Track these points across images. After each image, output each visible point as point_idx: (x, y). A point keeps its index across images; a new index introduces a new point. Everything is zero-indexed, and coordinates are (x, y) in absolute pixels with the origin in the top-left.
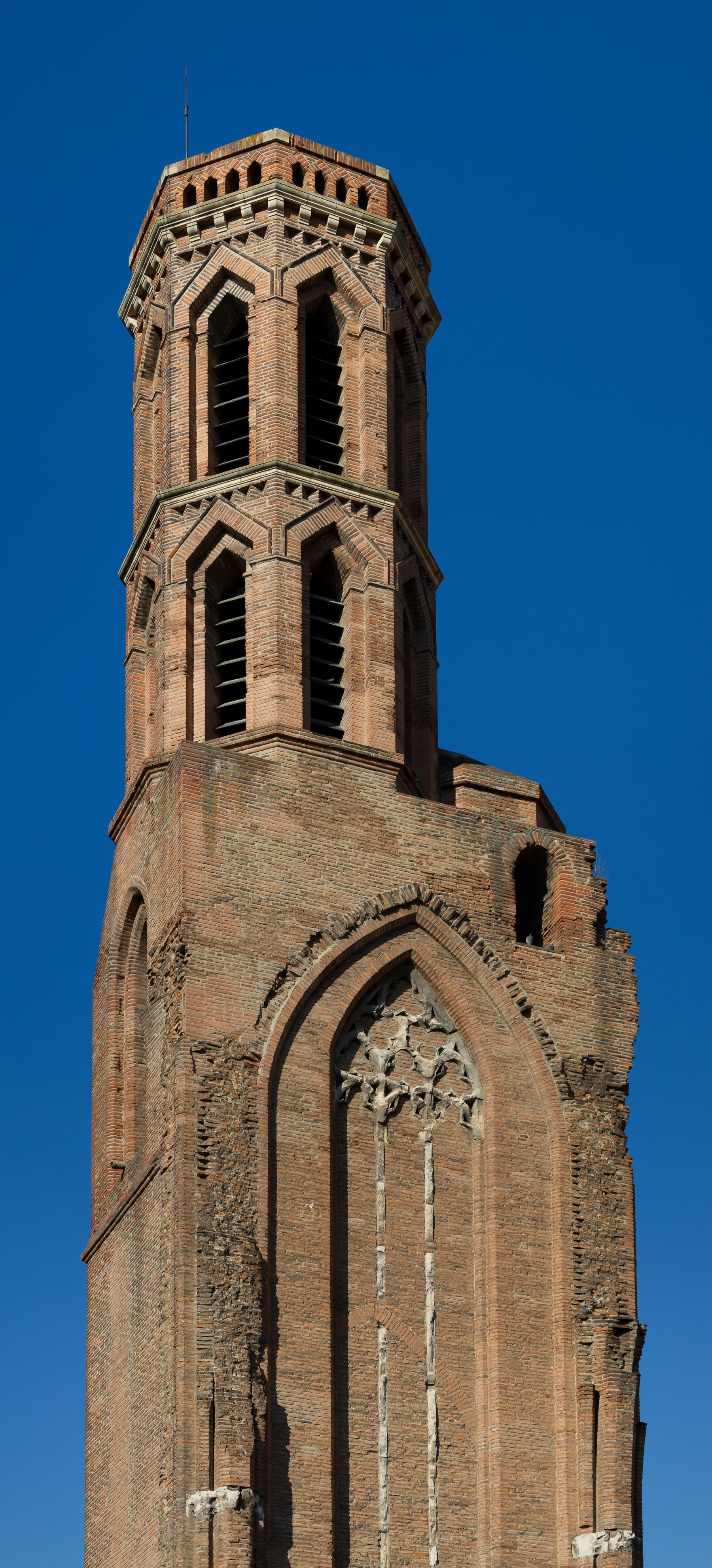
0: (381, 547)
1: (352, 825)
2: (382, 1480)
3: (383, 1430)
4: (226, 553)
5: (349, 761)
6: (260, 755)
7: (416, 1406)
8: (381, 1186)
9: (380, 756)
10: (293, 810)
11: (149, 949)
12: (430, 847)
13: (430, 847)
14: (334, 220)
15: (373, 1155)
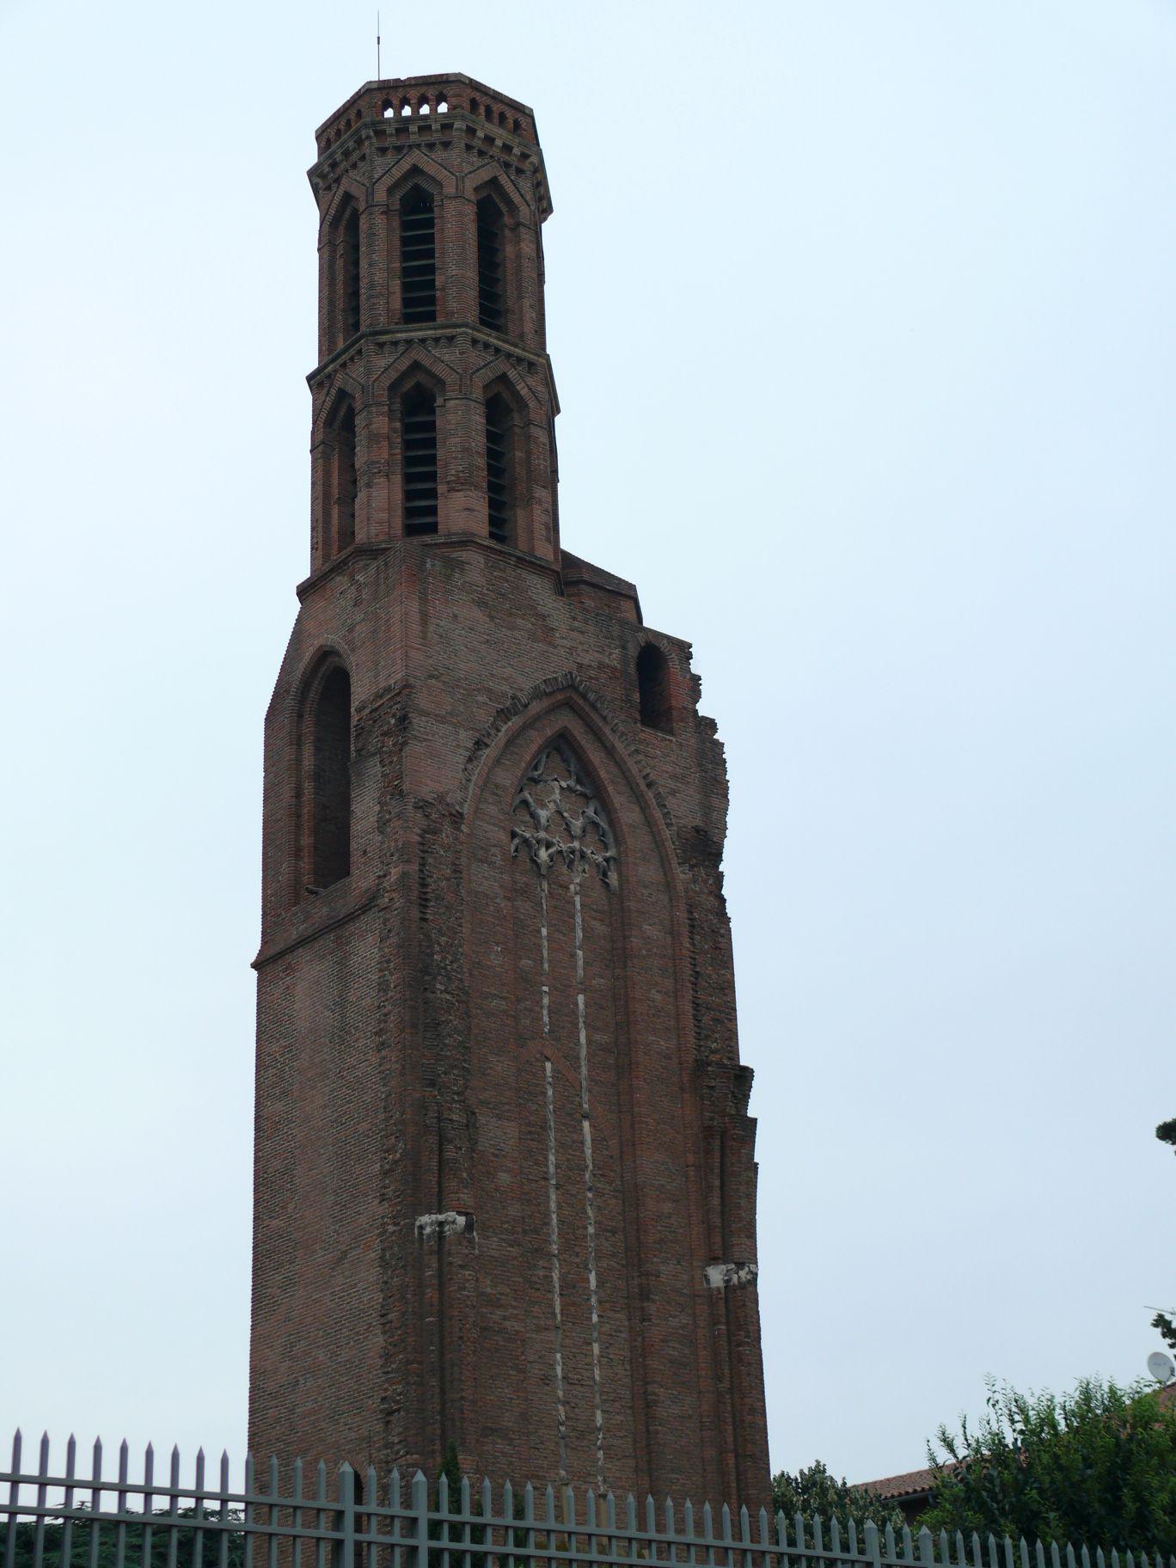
2: (553, 1206)
4: (418, 386)
6: (454, 555)
7: (575, 1136)
8: (544, 931)
10: (481, 603)
11: (354, 705)
14: (499, 143)
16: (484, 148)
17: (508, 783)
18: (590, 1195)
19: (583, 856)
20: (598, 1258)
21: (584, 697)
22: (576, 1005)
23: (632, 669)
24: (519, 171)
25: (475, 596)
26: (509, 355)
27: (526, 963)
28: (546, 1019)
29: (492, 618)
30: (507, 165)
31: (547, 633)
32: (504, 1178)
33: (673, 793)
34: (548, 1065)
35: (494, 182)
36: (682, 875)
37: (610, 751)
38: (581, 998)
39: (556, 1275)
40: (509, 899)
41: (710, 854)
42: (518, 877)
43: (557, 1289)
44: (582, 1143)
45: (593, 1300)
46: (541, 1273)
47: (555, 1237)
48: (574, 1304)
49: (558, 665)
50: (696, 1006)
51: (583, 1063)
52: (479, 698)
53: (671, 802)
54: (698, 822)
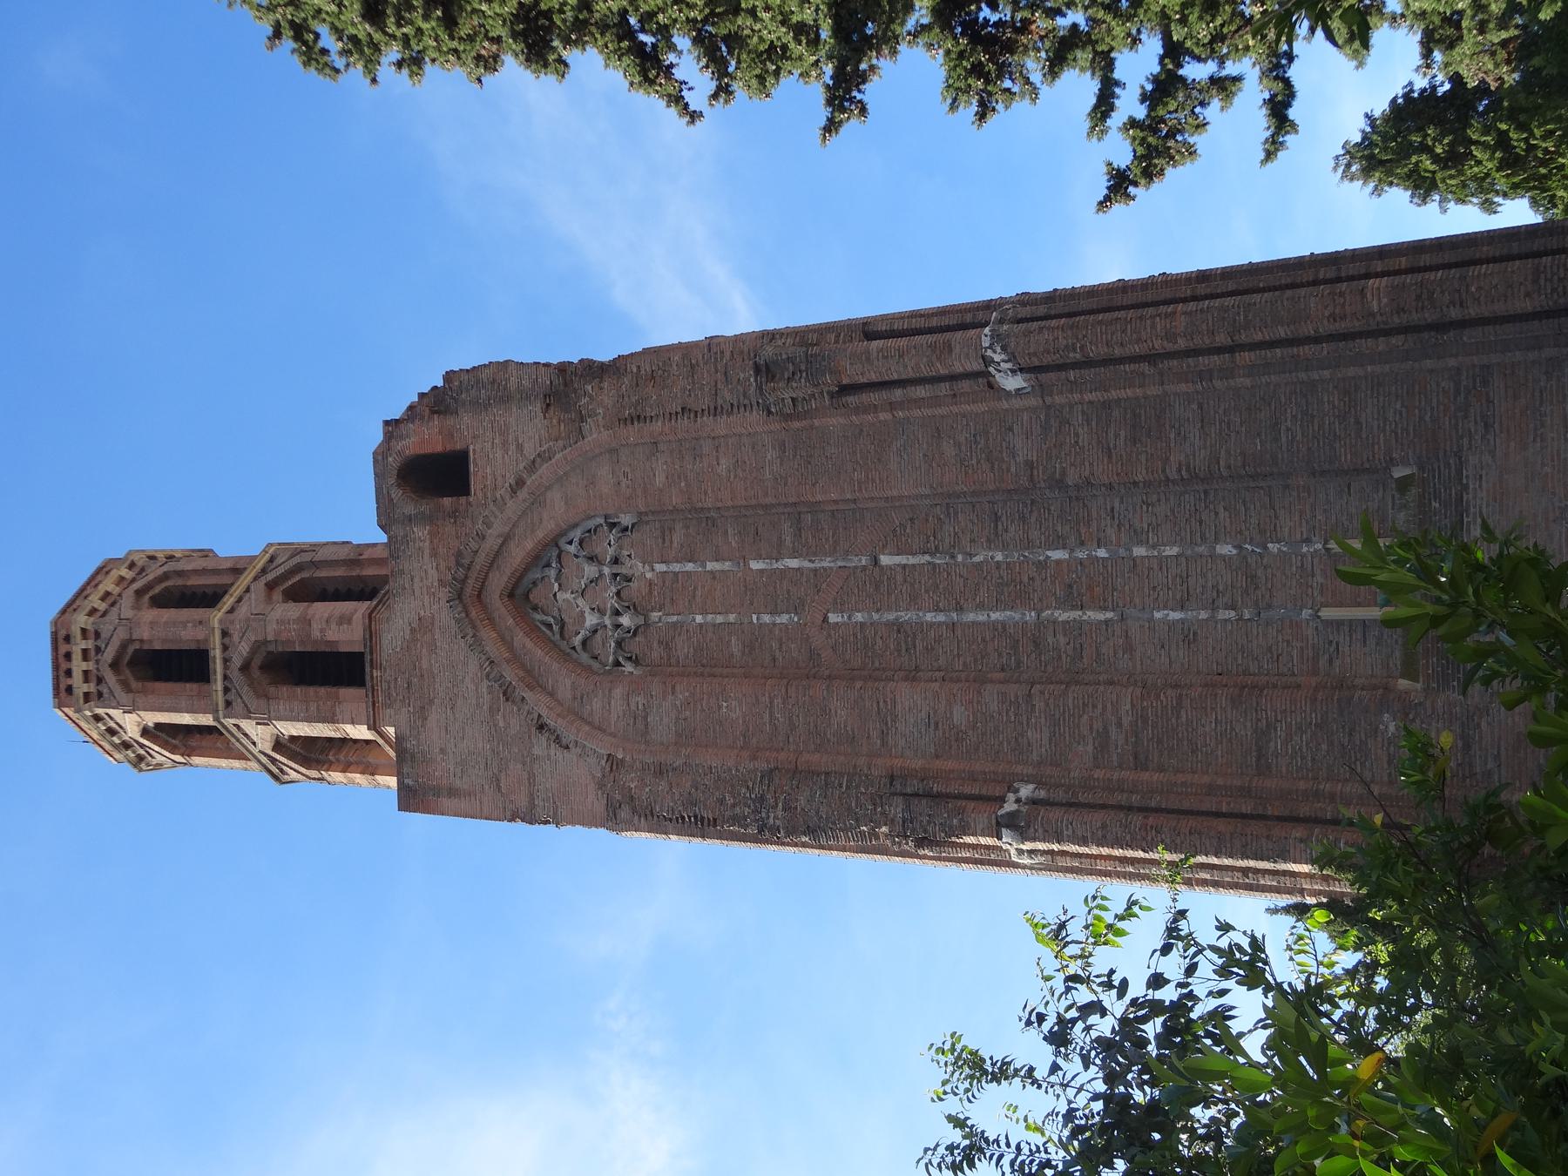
2: (981, 617)
3: (929, 617)
7: (899, 578)
8: (699, 619)
10: (422, 713)
14: (84, 666)
15: (674, 624)
17: (568, 682)
18: (960, 558)
19: (616, 561)
20: (1029, 545)
21: (463, 581)
22: (762, 571)
23: (425, 507)
24: (97, 635)
25: (419, 723)
26: (226, 661)
27: (735, 647)
28: (784, 619)
29: (431, 702)
30: (98, 650)
31: (423, 626)
32: (959, 715)
33: (520, 447)
34: (833, 618)
35: (115, 666)
36: (596, 435)
37: (507, 539)
38: (755, 565)
39: (1063, 616)
40: (673, 687)
41: (566, 385)
42: (655, 655)
43: (1076, 614)
44: (904, 567)
45: (1081, 554)
46: (1062, 640)
47: (1017, 616)
48: (1090, 588)
49: (445, 617)
50: (715, 411)
51: (817, 565)
52: (501, 724)
53: (530, 451)
54: (538, 407)
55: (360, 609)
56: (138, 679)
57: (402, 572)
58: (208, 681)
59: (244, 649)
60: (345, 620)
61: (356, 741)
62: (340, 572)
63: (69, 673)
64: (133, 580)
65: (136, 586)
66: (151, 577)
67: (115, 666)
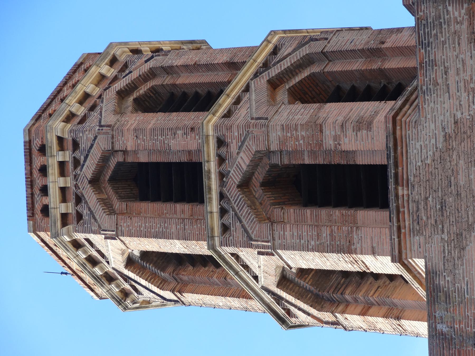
0: (242, 138)
1: (458, 174)
5: (405, 177)
9: (391, 145)
10: (459, 242)
12: (457, 78)
13: (457, 78)
14: (61, 182)
16: (72, 198)
24: (76, 145)
25: (456, 254)
26: (222, 176)
30: (76, 163)
55: (381, 110)
56: (121, 198)
57: (434, 63)
58: (202, 201)
59: (243, 161)
60: (364, 124)
61: (377, 276)
62: (357, 65)
63: (45, 190)
64: (115, 79)
65: (119, 85)
66: (135, 75)
67: (95, 181)
